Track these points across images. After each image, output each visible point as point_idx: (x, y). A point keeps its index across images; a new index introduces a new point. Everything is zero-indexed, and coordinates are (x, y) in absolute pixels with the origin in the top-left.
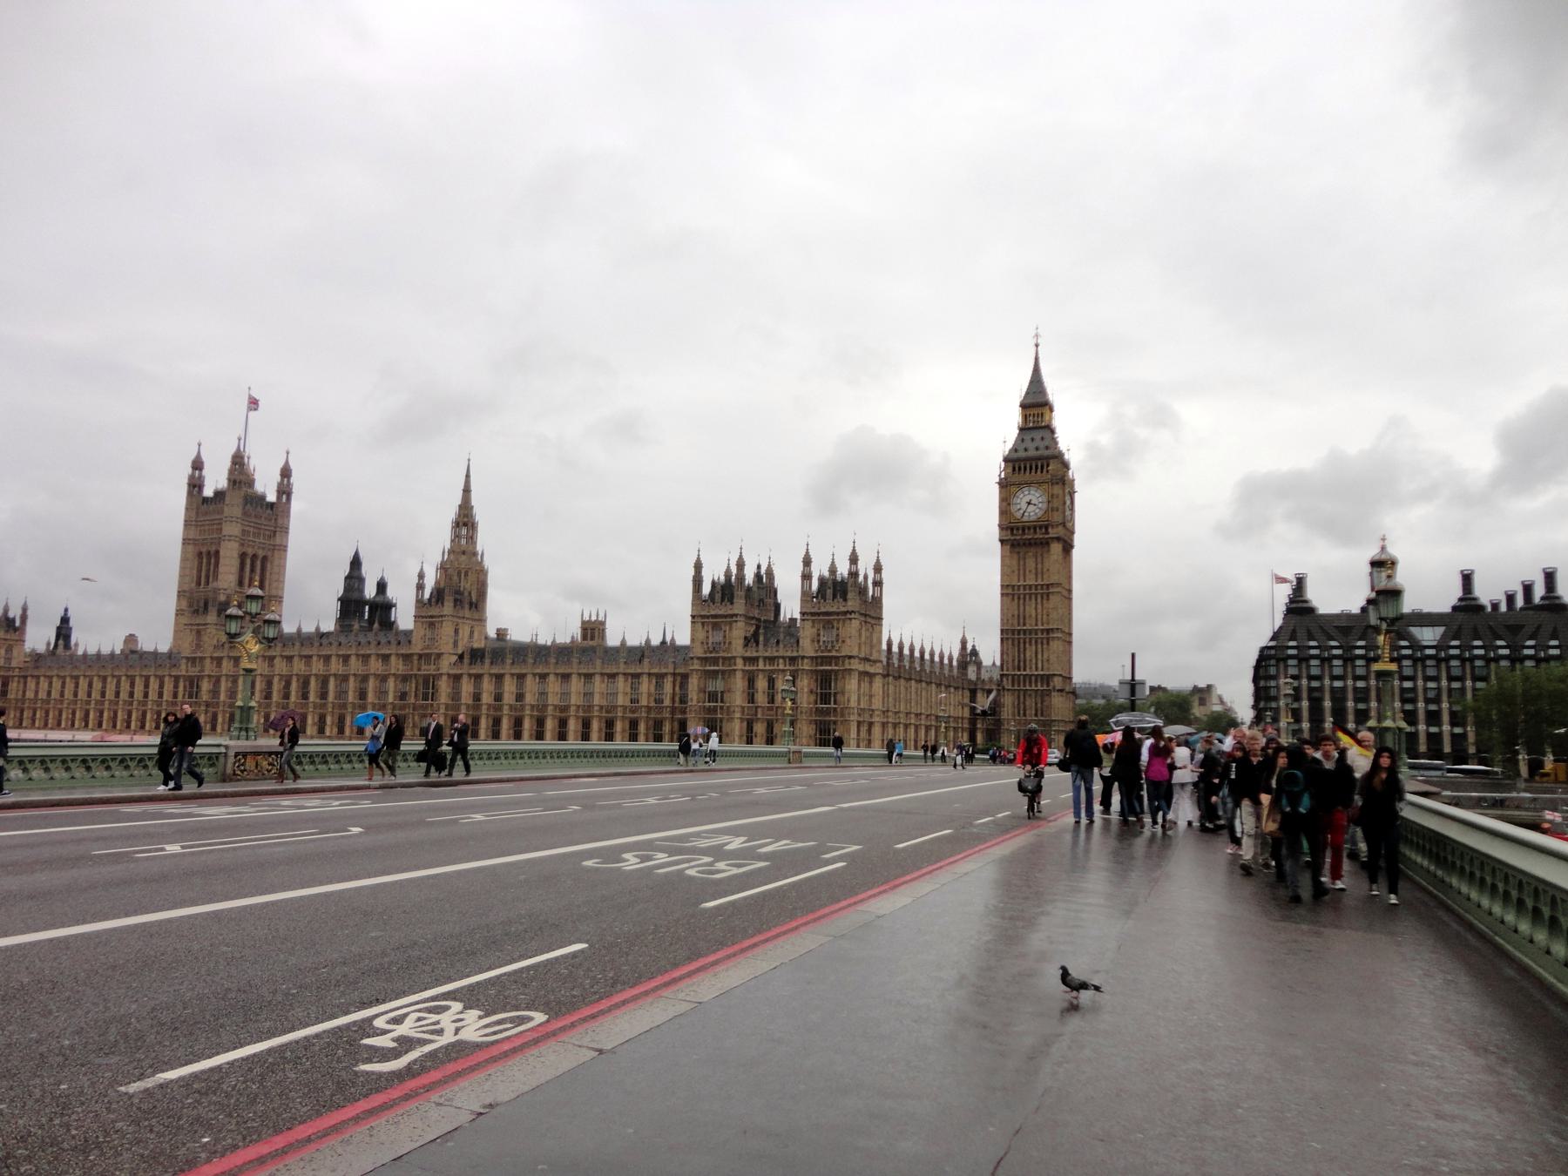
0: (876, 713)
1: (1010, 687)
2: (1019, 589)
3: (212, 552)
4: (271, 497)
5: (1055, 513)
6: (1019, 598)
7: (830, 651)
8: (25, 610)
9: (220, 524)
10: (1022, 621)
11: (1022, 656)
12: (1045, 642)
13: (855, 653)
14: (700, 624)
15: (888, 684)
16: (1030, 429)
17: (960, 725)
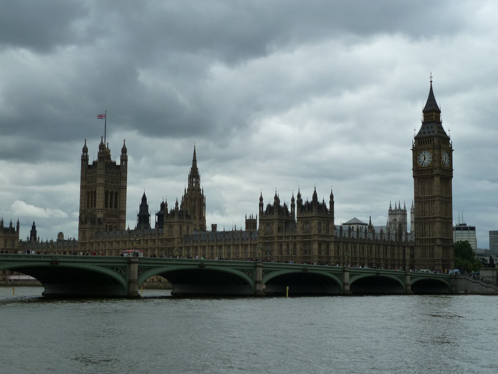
0: (332, 257)
1: (419, 245)
2: (422, 199)
3: (93, 191)
4: (118, 163)
5: (435, 163)
6: (422, 203)
7: (307, 233)
8: (18, 223)
9: (96, 178)
10: (423, 214)
11: (424, 230)
12: (433, 223)
13: (317, 232)
14: (262, 223)
15: (341, 245)
16: (426, 123)
17: (397, 263)
